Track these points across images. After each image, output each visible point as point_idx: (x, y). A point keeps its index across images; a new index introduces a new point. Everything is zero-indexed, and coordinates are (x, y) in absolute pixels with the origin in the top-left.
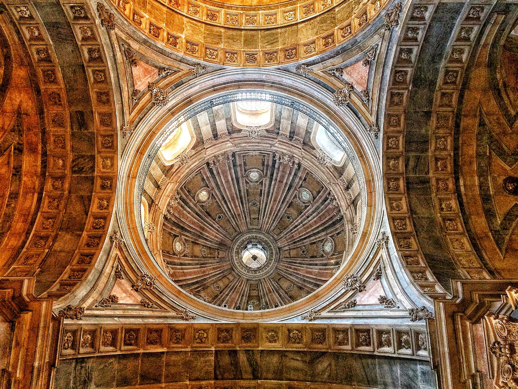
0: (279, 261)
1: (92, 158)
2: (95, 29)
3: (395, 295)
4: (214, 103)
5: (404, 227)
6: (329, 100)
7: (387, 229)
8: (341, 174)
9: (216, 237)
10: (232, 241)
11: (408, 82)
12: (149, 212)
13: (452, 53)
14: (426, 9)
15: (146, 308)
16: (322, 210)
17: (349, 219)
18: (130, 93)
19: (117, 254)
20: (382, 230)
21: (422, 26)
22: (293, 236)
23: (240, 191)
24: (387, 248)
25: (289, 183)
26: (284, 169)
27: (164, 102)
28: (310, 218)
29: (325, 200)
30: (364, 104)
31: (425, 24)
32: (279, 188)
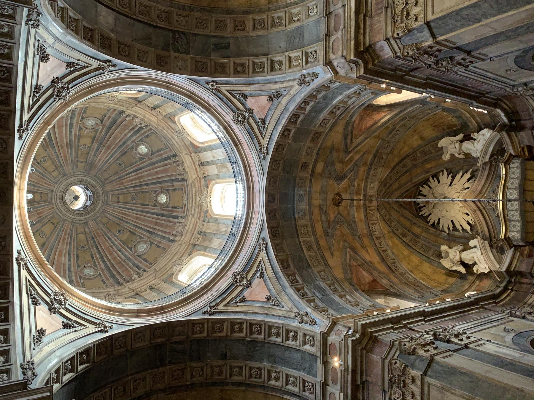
0: (73, 222)
1: (187, 52)
2: (298, 68)
3: (47, 345)
4: (234, 166)
5: (118, 347)
6: (237, 267)
7: (116, 330)
8: (165, 281)
9: (100, 160)
10: (95, 176)
11: (252, 336)
12: (129, 98)
13: (276, 372)
14: (312, 346)
15: (33, 90)
16: (128, 265)
17: (120, 291)
18: (245, 93)
19: (92, 65)
20: (114, 326)
21: (298, 344)
22: (99, 236)
23: (147, 184)
24: (96, 332)
25: (156, 232)
26: (170, 227)
27: (237, 121)
28: (119, 252)
29: (137, 267)
30: (233, 299)
31: (300, 346)
32: (151, 222)
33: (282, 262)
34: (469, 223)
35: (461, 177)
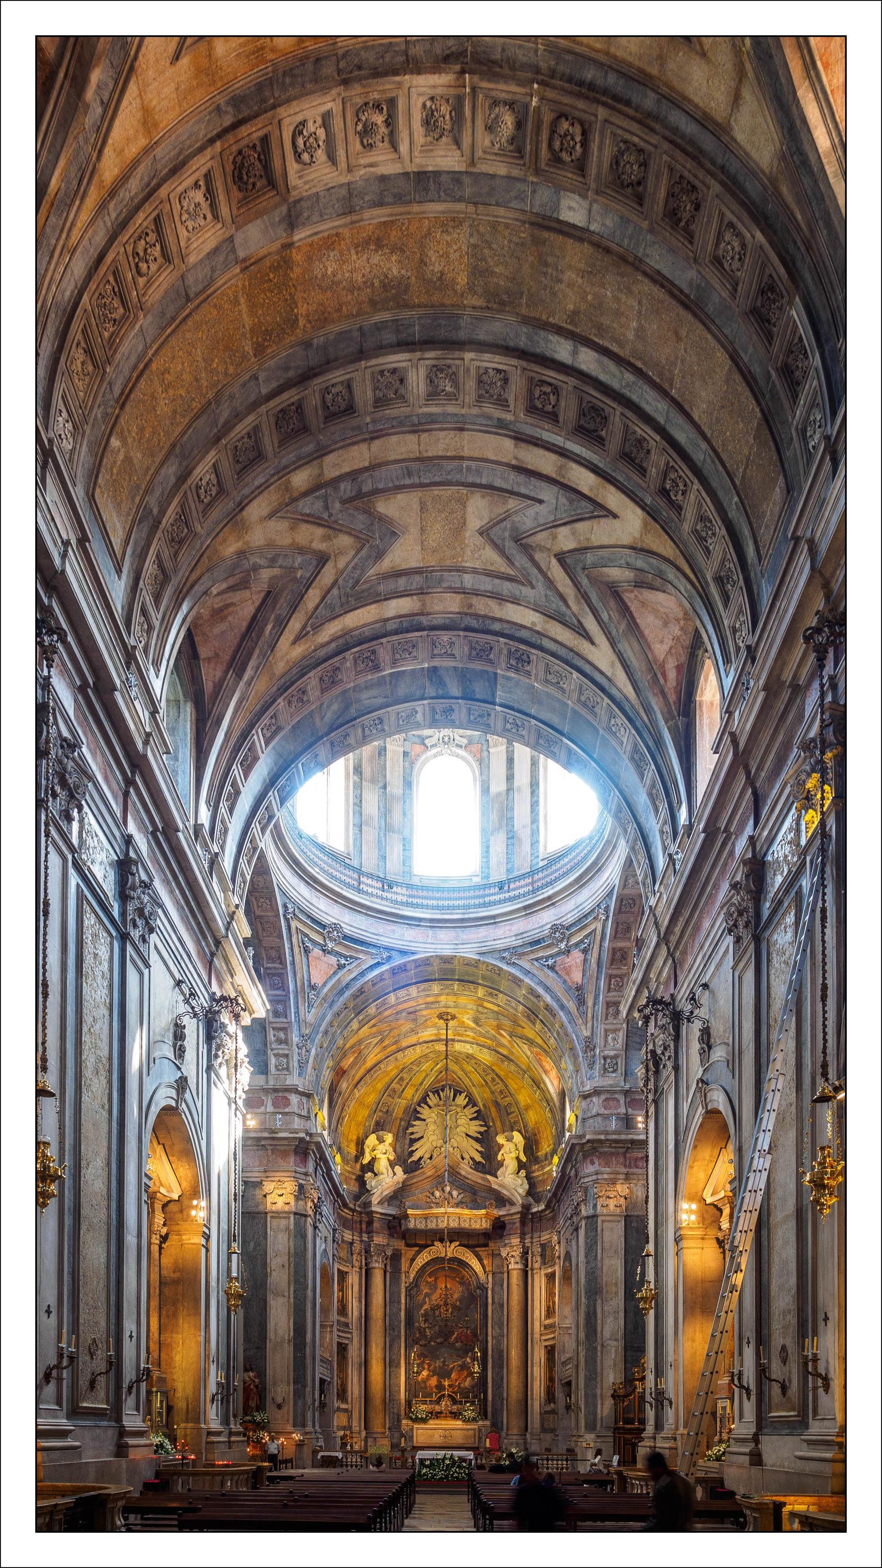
33: (361, 991)
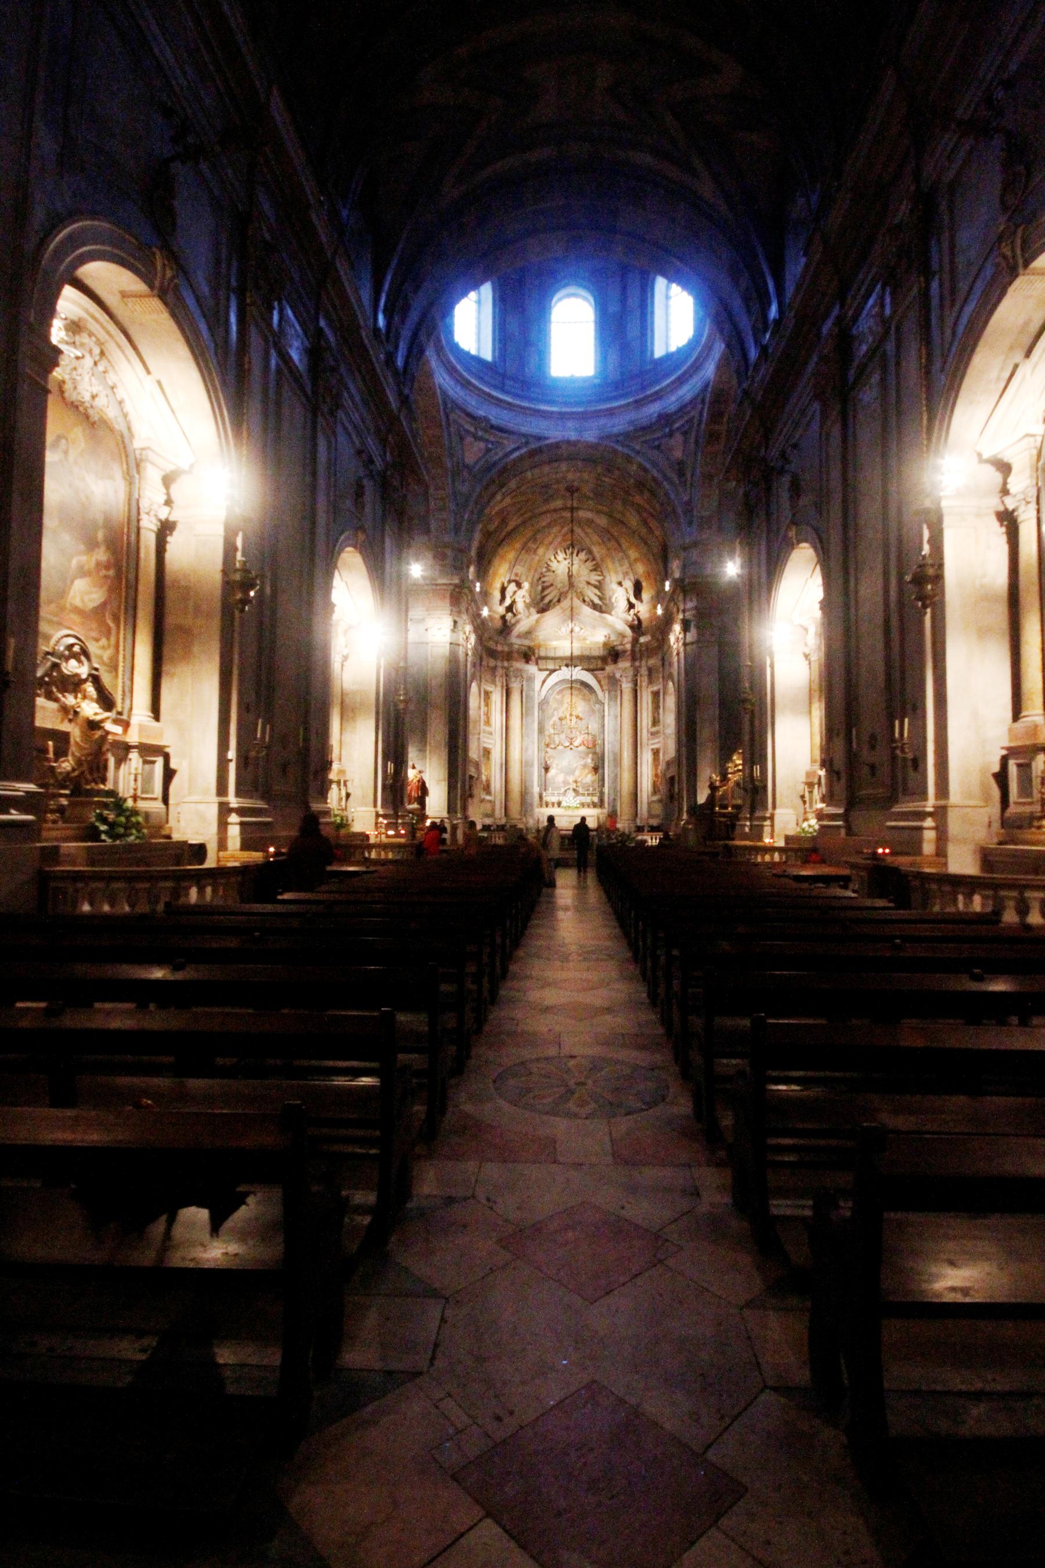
34: (551, 601)
35: (596, 594)
